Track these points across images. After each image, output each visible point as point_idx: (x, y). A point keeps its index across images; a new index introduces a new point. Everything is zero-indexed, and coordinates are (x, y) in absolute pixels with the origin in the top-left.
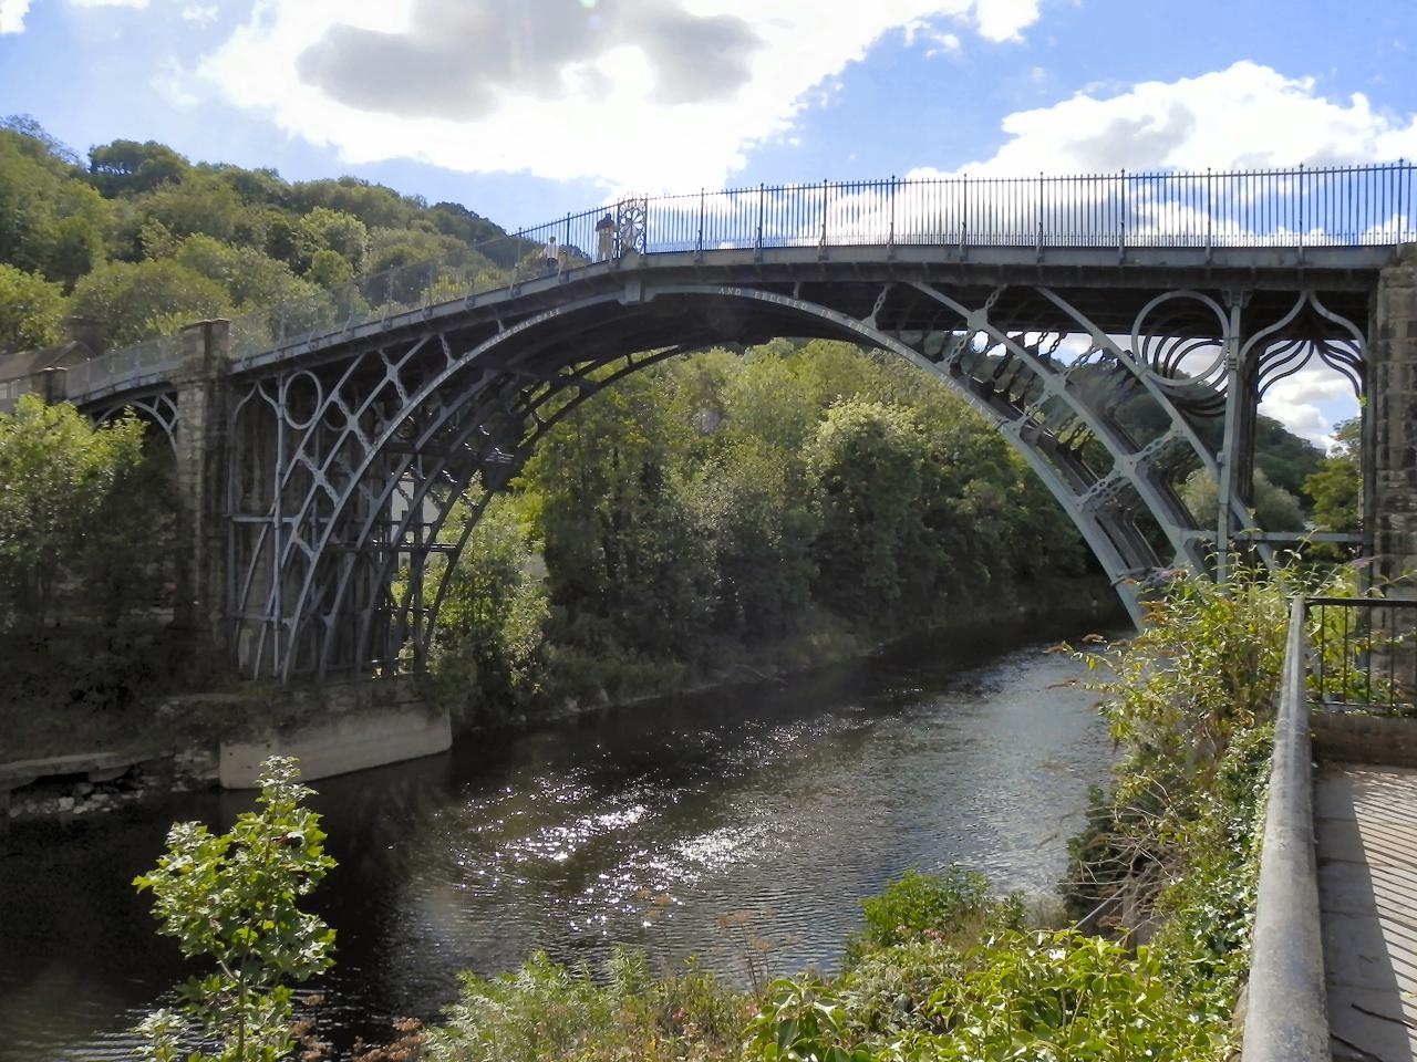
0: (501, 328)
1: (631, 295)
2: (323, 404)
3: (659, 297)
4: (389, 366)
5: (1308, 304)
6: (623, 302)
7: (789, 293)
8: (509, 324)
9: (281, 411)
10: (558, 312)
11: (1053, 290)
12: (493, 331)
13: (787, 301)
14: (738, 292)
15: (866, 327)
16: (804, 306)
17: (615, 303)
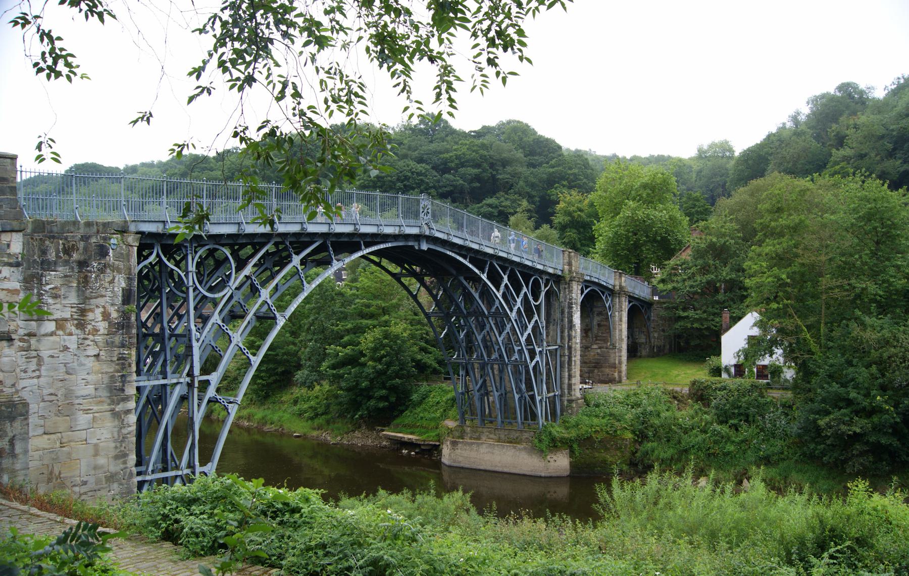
0: (363, 247)
1: (425, 247)
2: (236, 278)
3: (428, 249)
4: (294, 256)
5: (551, 286)
6: (417, 248)
7: (465, 257)
8: (368, 245)
9: (191, 280)
10: (389, 245)
11: (519, 271)
12: (360, 249)
13: (466, 262)
14: (453, 255)
15: (484, 277)
16: (471, 266)
17: (412, 247)
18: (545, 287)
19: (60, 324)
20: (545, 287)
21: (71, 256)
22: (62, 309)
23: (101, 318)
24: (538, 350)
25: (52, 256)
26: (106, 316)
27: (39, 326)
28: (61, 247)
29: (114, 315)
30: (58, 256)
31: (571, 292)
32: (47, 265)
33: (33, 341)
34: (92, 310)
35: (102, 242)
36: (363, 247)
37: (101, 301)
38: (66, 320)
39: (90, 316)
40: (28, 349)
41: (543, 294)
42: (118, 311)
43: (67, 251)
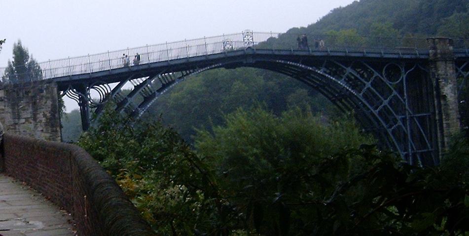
1: (251, 61)
7: (297, 62)
8: (202, 67)
18: (406, 71)
19: (27, 119)
20: (406, 71)
21: (28, 95)
22: (27, 114)
23: (42, 116)
24: (399, 117)
25: (21, 94)
26: (45, 115)
27: (19, 120)
28: (24, 92)
29: (48, 115)
30: (24, 96)
31: (436, 68)
32: (20, 99)
33: (17, 126)
34: (39, 114)
35: (40, 88)
36: (197, 68)
37: (42, 110)
38: (29, 118)
39: (38, 116)
40: (15, 129)
41: (404, 76)
42: (49, 113)
43: (27, 93)
